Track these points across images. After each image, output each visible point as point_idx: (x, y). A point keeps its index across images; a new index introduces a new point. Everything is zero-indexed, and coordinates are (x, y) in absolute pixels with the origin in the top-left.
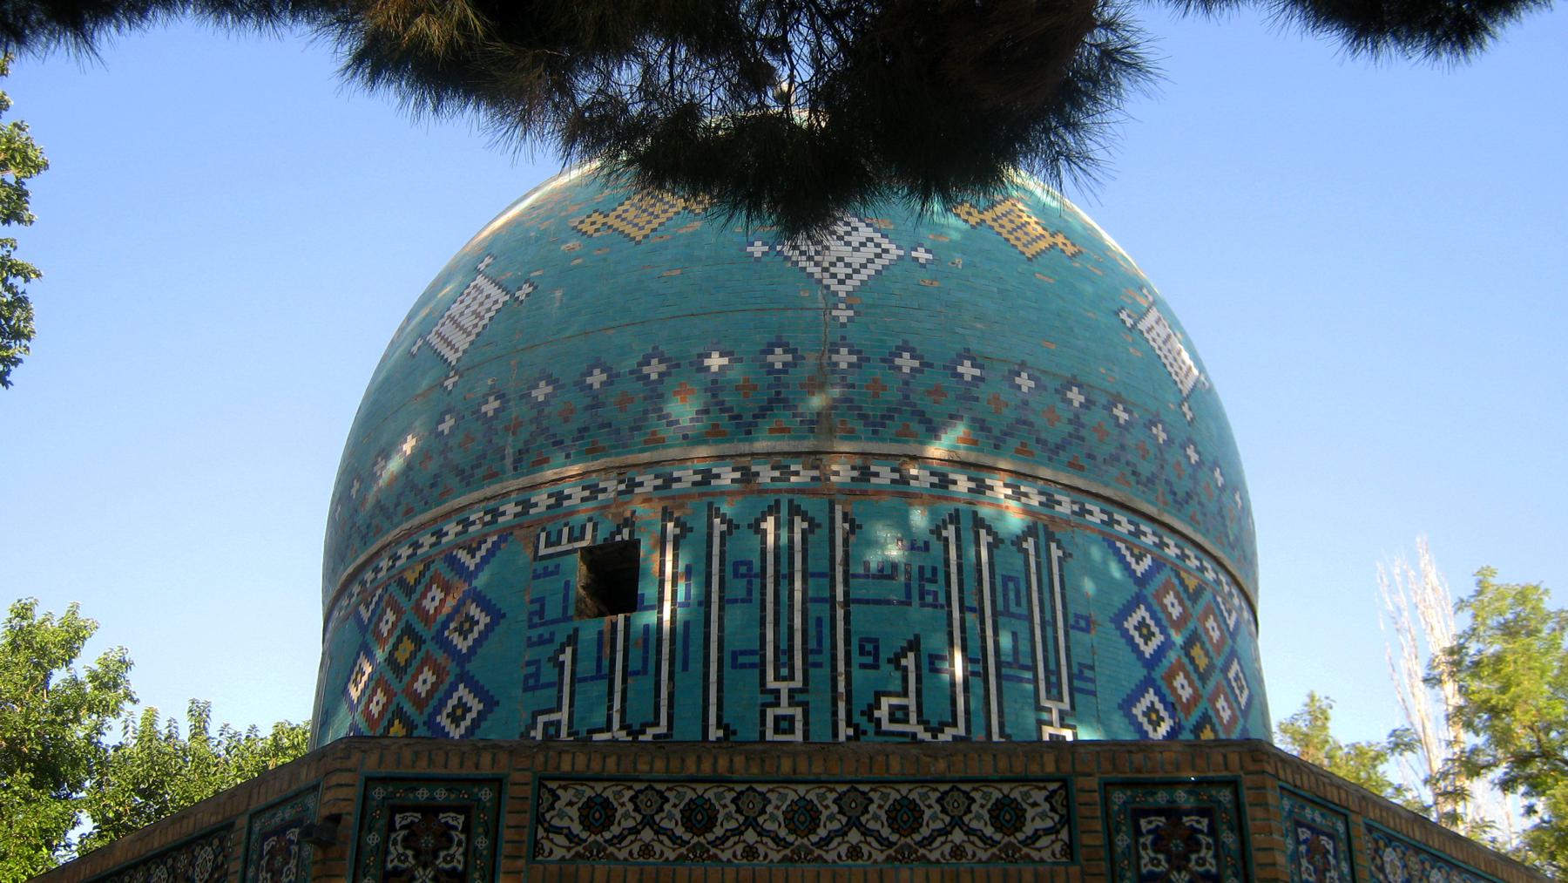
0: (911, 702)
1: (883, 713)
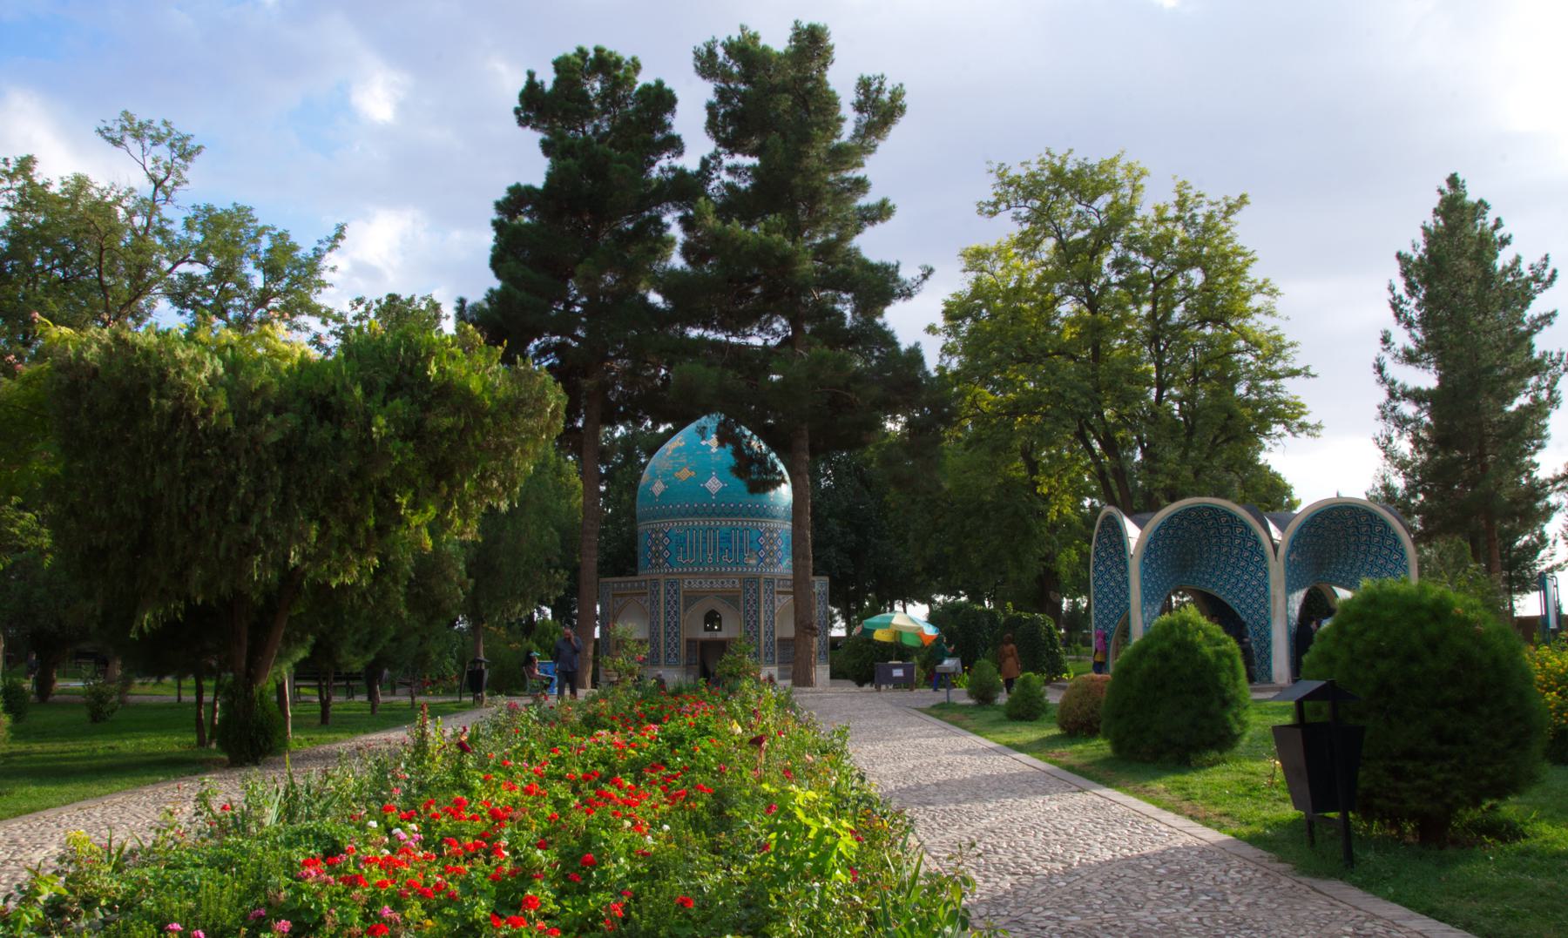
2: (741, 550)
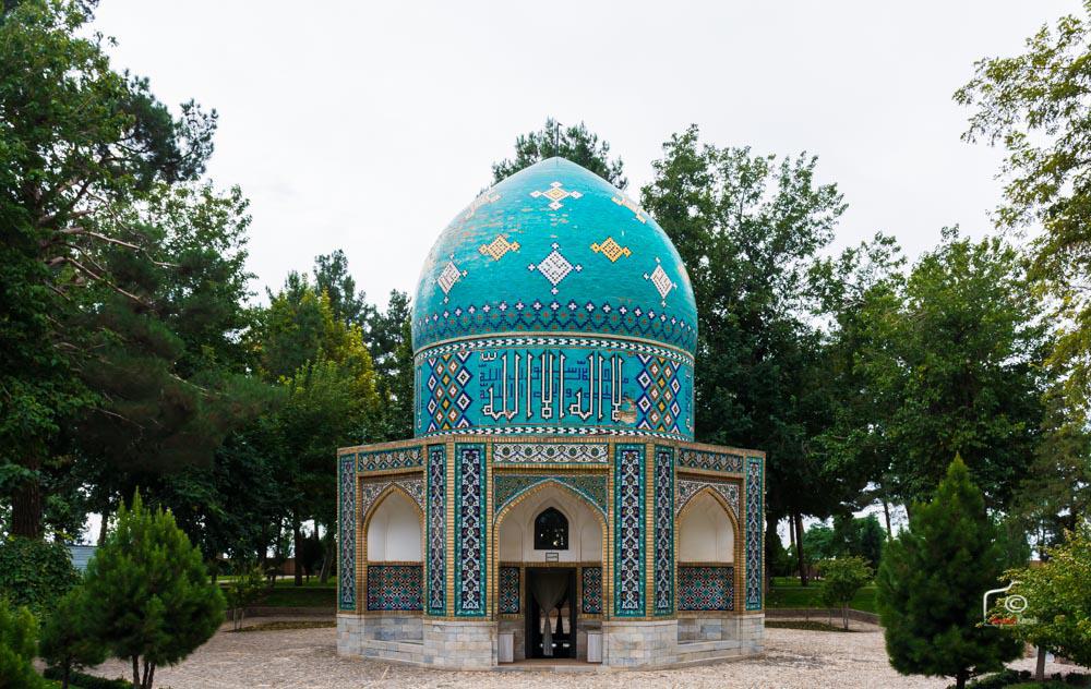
0: (579, 406)
1: (571, 409)
2: (607, 396)
